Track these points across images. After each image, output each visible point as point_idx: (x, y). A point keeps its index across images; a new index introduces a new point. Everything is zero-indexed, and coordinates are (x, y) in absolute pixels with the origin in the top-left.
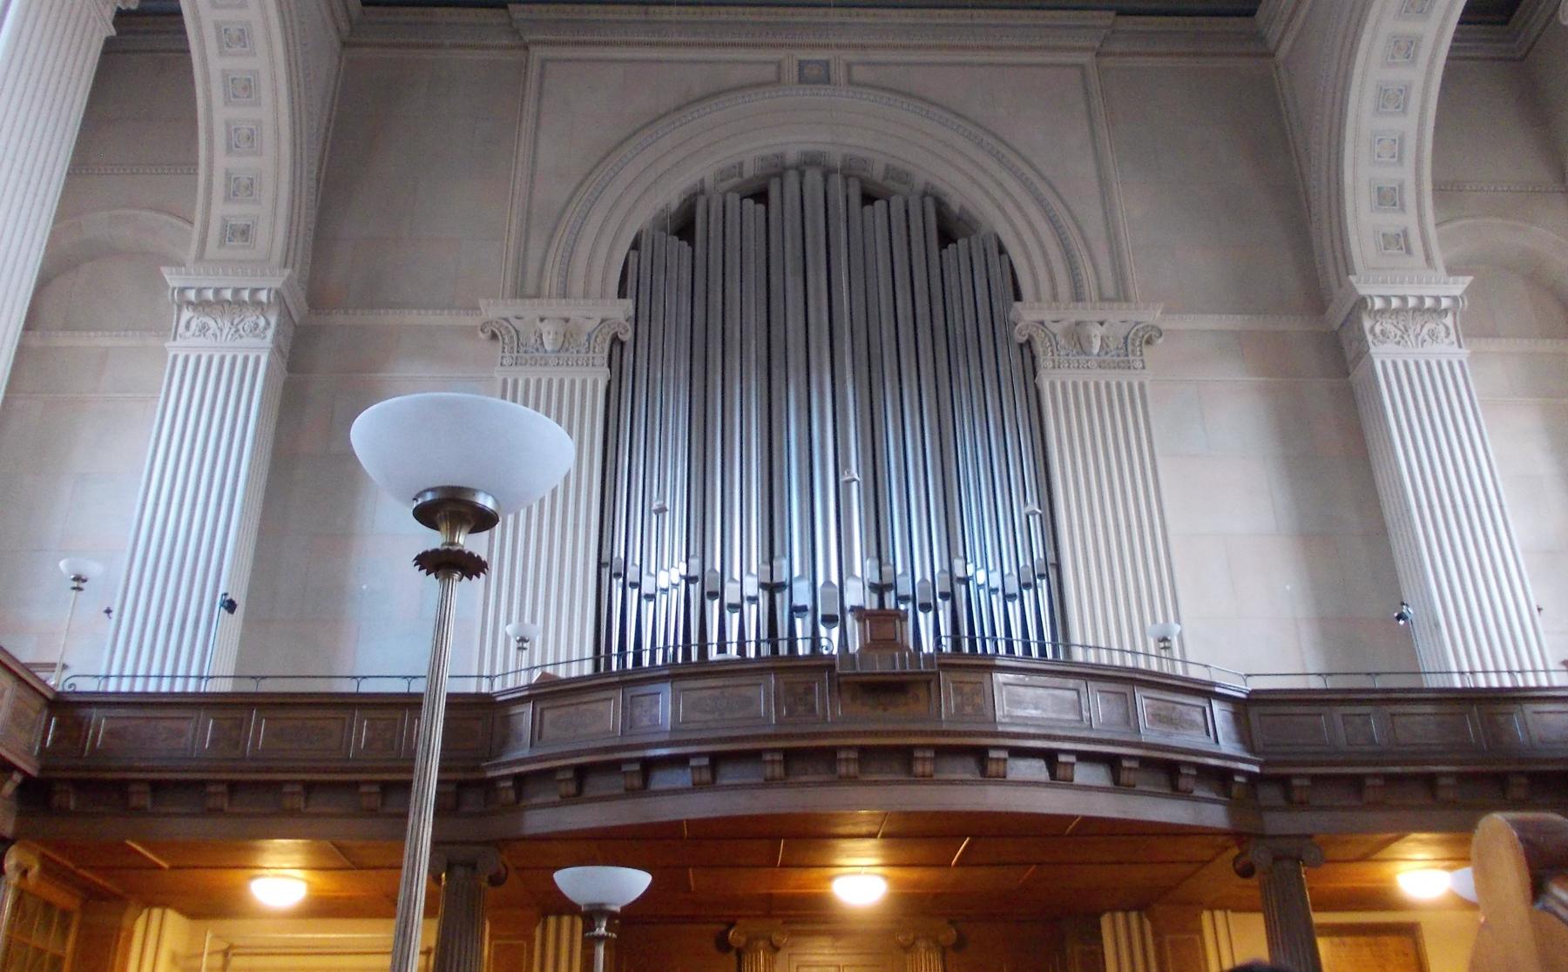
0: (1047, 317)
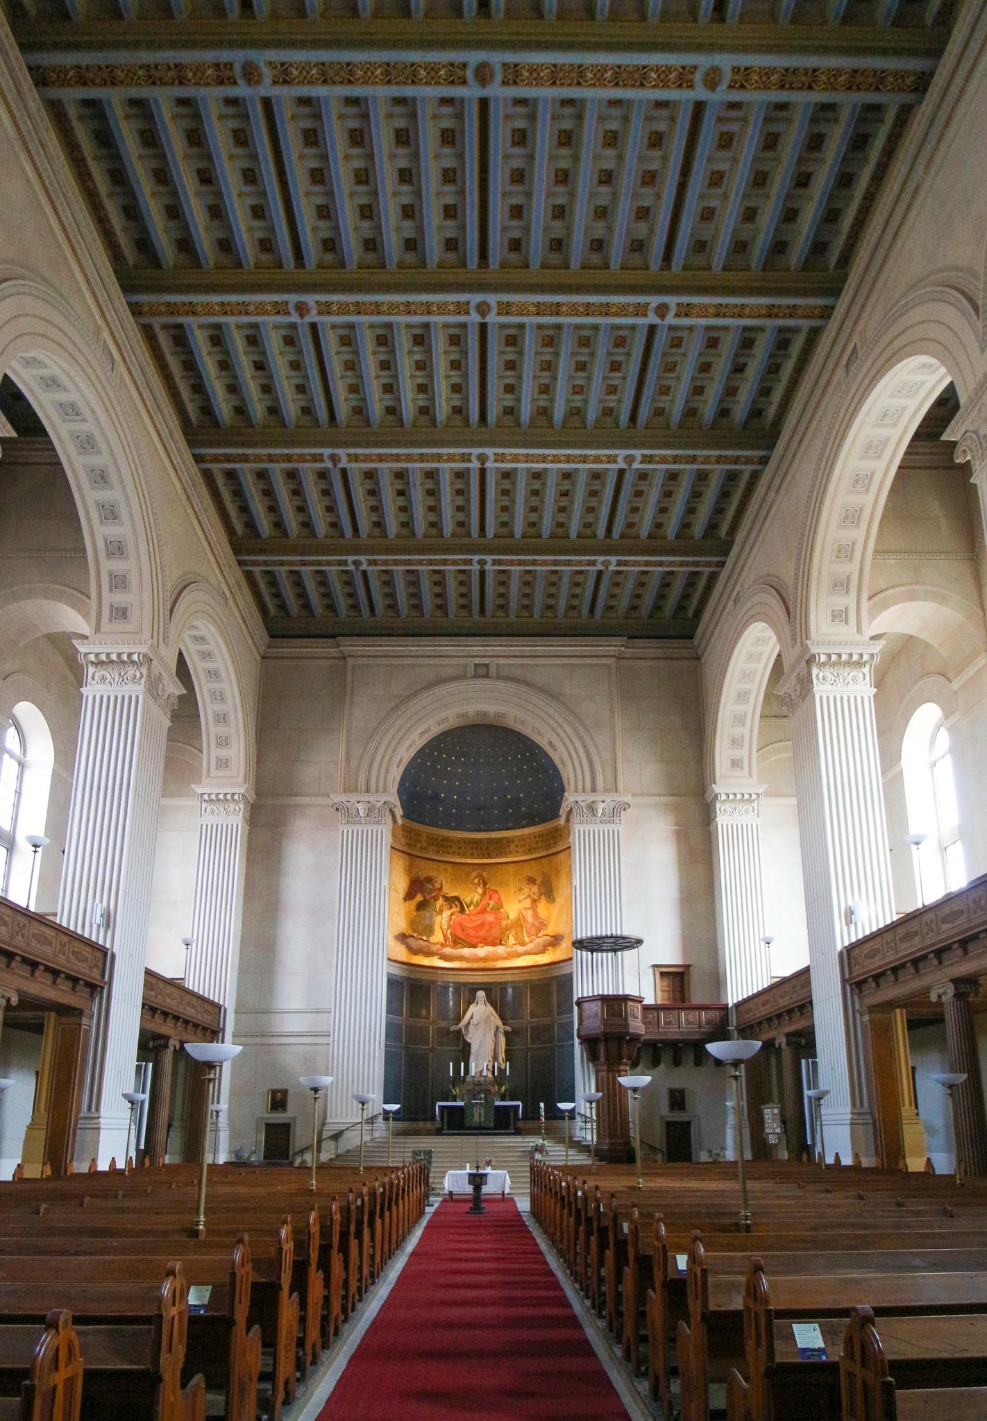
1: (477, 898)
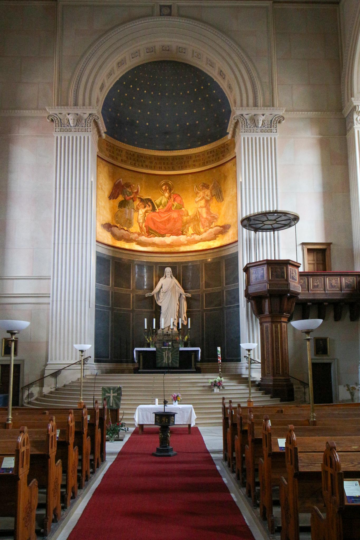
0: (244, 113)
1: (164, 200)
